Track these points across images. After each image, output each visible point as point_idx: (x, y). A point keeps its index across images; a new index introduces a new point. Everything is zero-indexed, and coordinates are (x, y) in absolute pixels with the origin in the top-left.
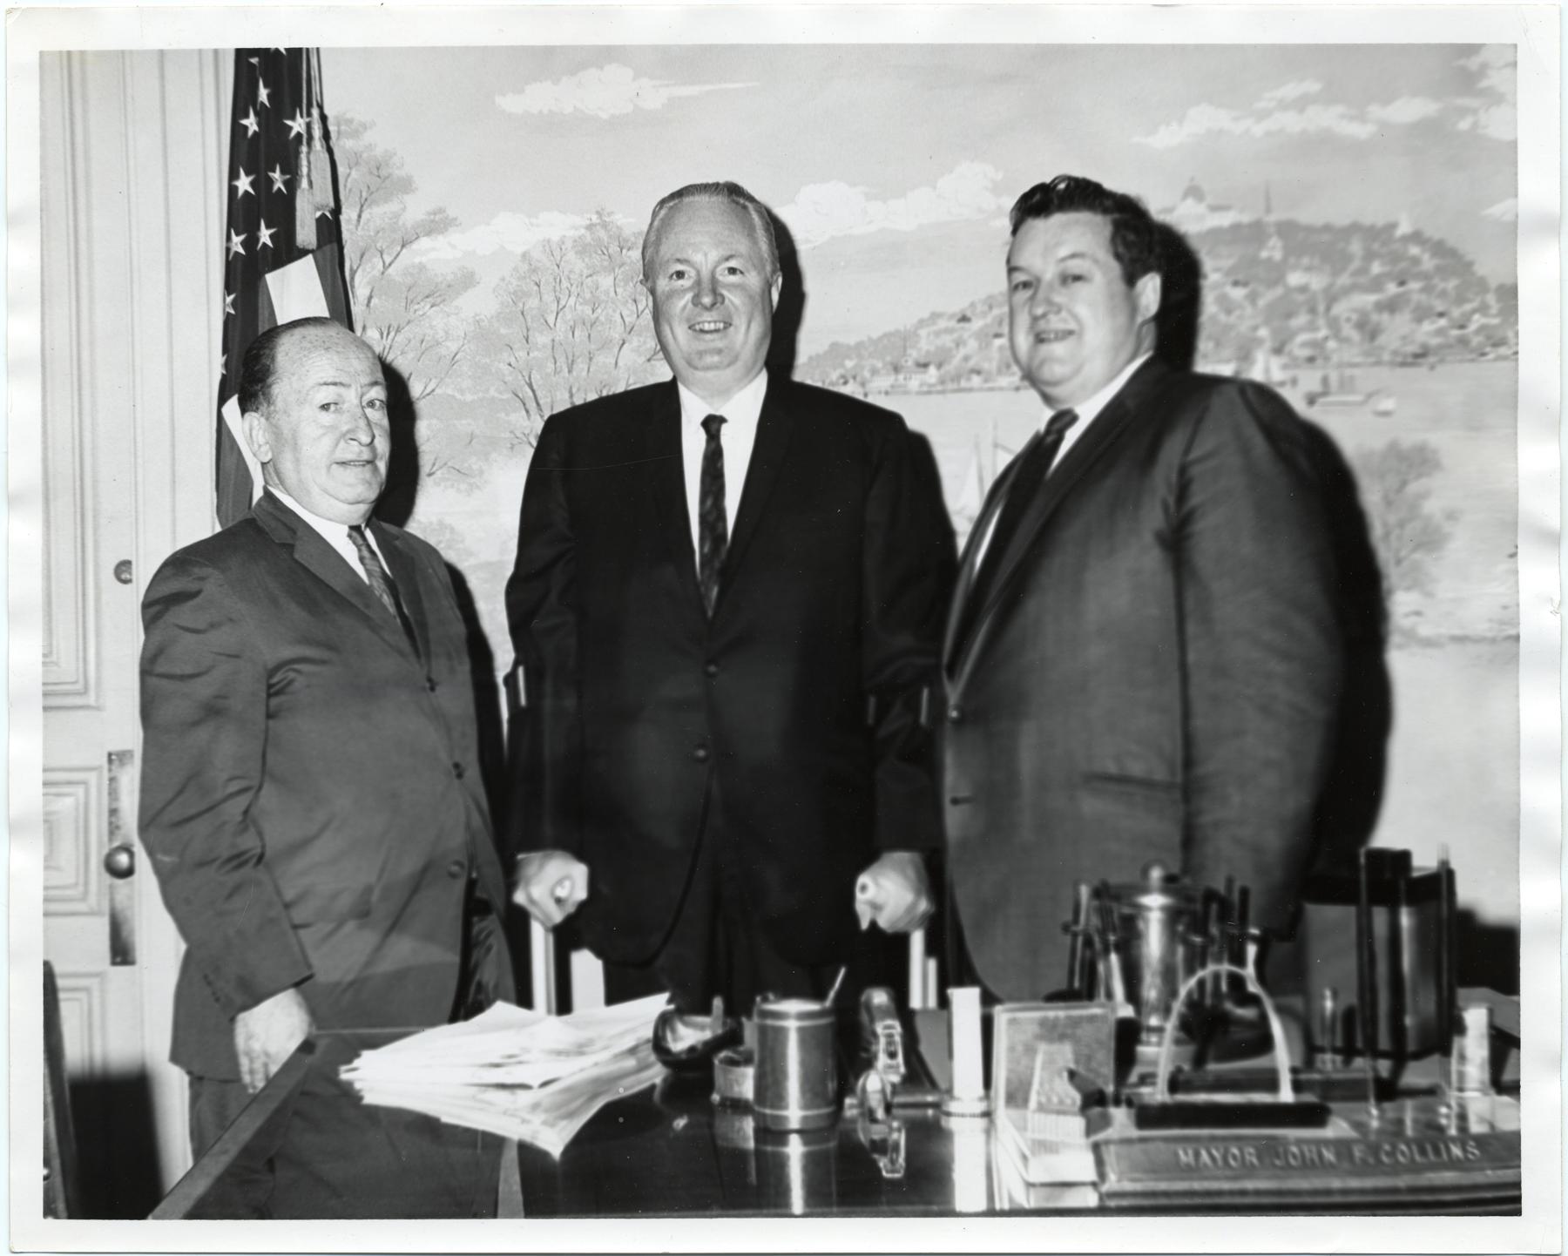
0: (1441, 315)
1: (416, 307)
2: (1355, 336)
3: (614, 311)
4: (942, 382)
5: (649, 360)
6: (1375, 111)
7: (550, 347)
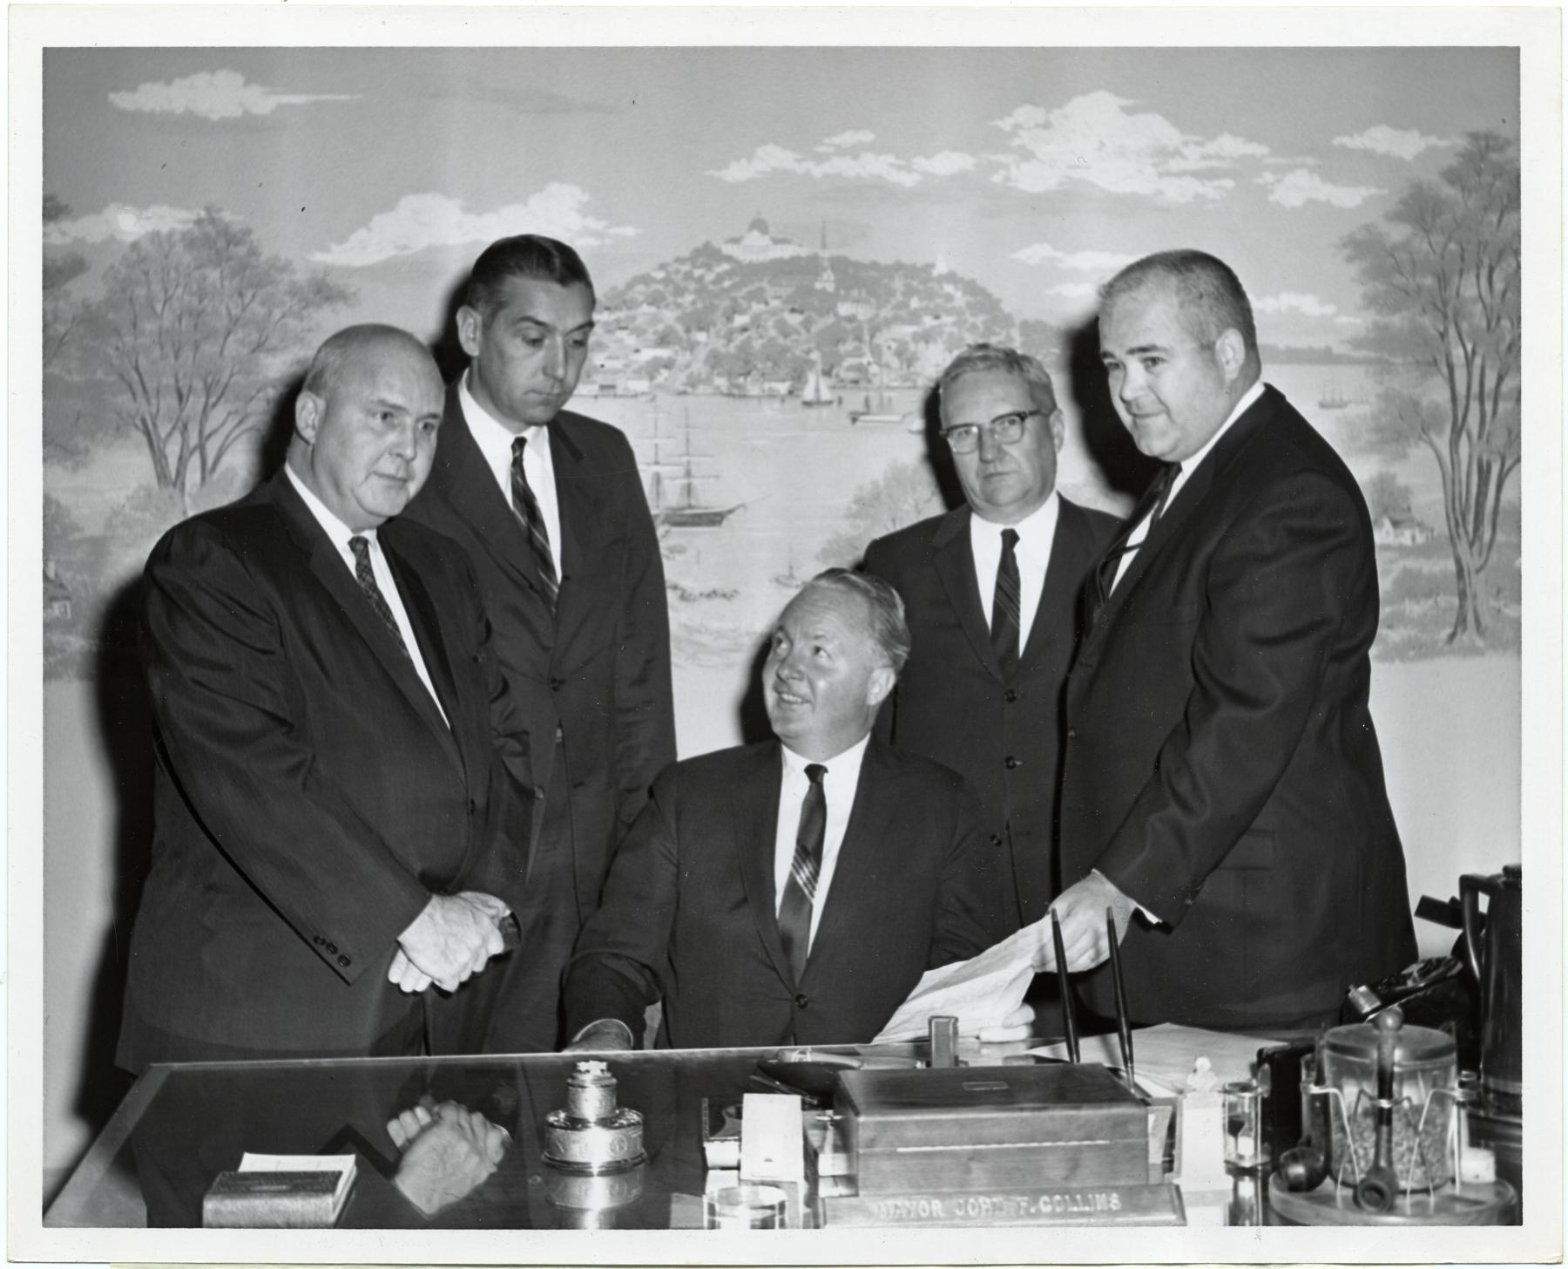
2: (895, 363)
5: (254, 351)
6: (920, 162)
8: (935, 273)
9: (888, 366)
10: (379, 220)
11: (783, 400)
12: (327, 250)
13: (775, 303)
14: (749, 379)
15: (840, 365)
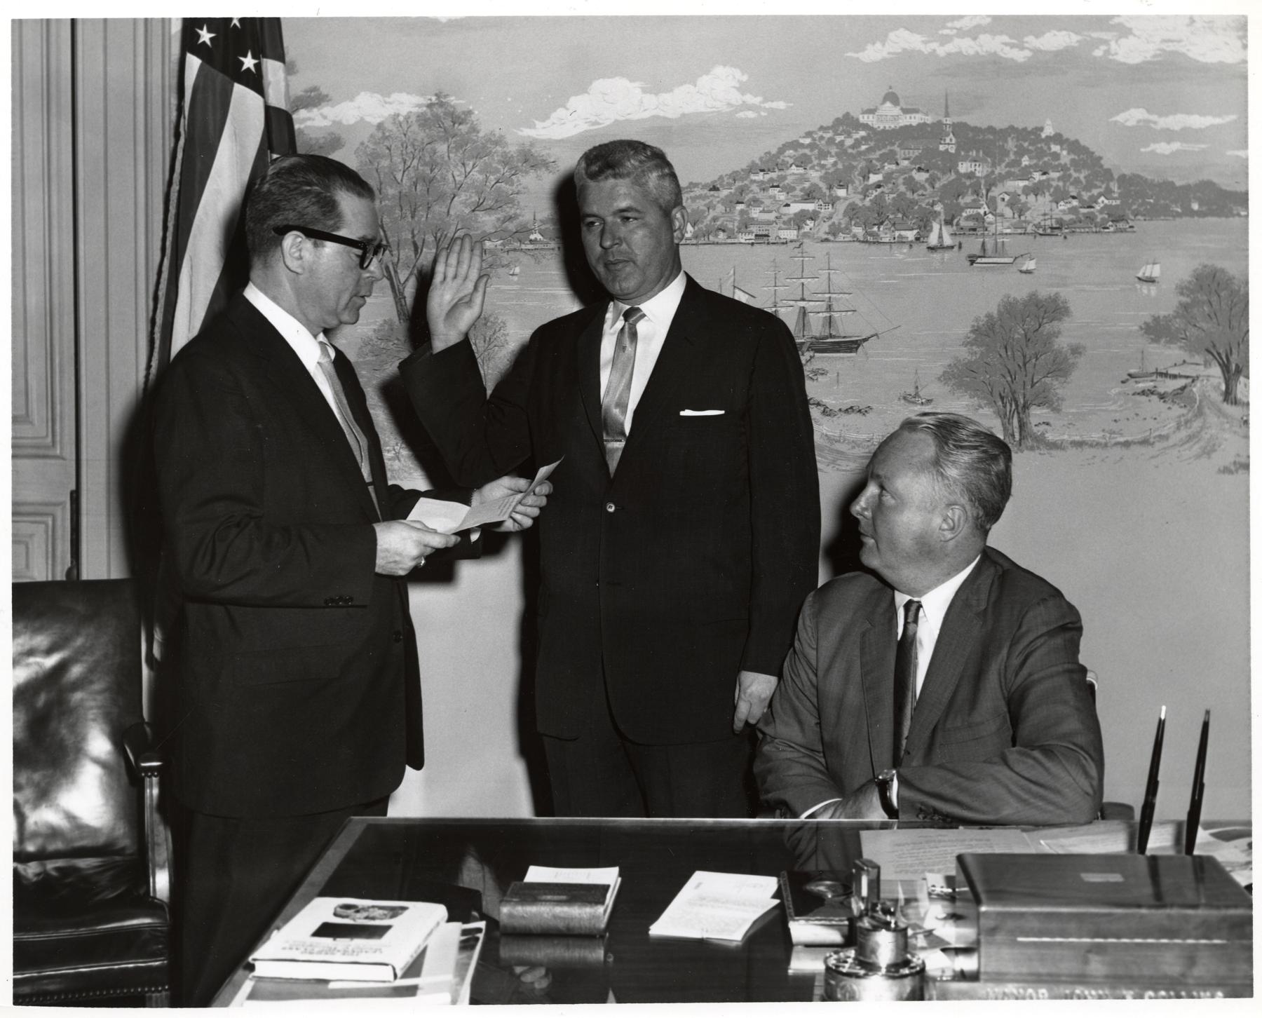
0: (1074, 197)
2: (1008, 212)
3: (447, 172)
4: (696, 236)
5: (473, 211)
6: (1031, 41)
7: (398, 198)
8: (1043, 135)
9: (1002, 215)
10: (574, 102)
11: (911, 246)
12: (532, 126)
13: (906, 163)
14: (881, 229)
15: (961, 216)
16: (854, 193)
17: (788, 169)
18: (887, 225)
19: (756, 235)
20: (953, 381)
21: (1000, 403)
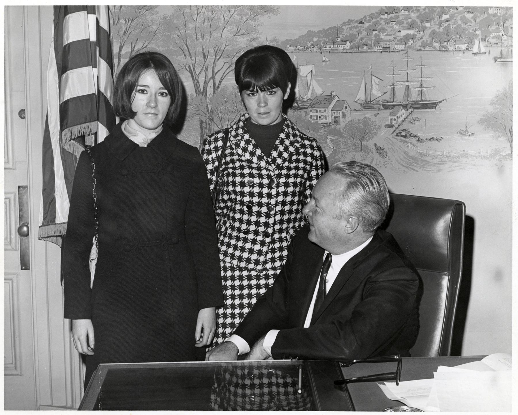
1: (140, 11)
3: (221, 15)
11: (464, 52)
14: (448, 44)
15: (490, 36)
16: (435, 25)
17: (400, 12)
18: (451, 41)
19: (383, 48)
20: (485, 124)
21: (509, 135)
